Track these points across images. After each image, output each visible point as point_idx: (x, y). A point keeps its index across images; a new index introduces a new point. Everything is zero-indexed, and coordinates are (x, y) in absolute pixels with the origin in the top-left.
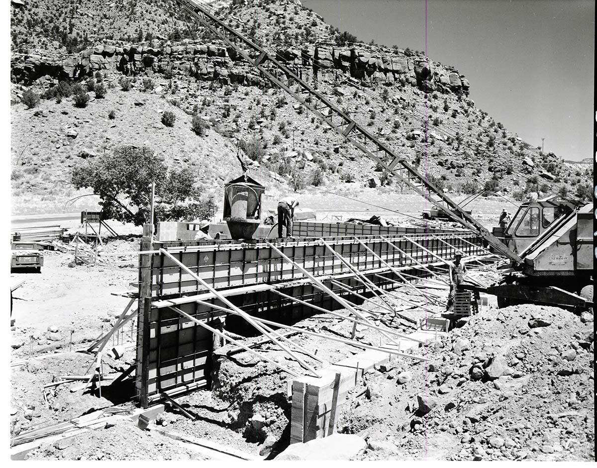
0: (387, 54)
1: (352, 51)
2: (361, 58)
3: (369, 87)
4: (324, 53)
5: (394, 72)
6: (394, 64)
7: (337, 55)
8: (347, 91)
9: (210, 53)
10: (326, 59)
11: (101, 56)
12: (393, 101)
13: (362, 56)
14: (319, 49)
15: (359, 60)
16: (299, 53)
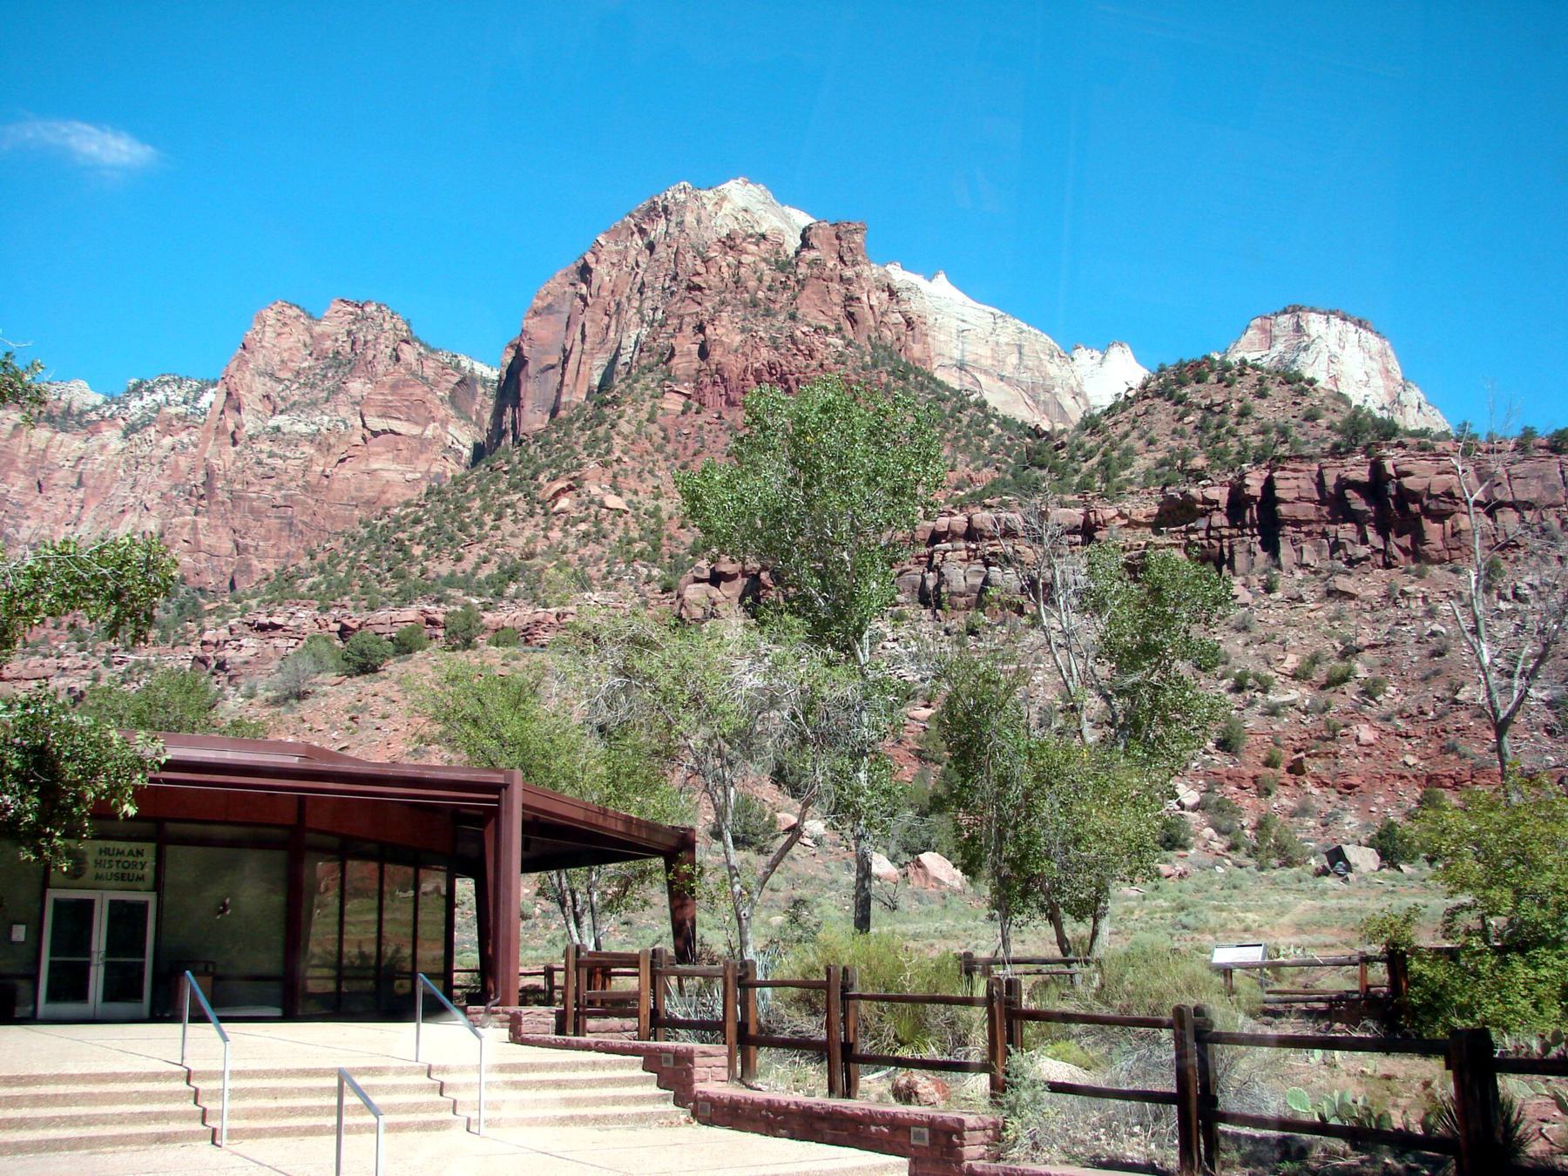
0: (1491, 457)
1: (1377, 468)
2: (1406, 482)
3: (1441, 561)
4: (1293, 483)
5: (1515, 506)
6: (1516, 483)
7: (1330, 481)
8: (1369, 584)
9: (972, 534)
10: (1299, 499)
11: (707, 585)
12: (1515, 595)
13: (1408, 474)
14: (1276, 474)
15: (1399, 487)
16: (1220, 494)
